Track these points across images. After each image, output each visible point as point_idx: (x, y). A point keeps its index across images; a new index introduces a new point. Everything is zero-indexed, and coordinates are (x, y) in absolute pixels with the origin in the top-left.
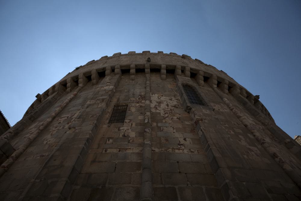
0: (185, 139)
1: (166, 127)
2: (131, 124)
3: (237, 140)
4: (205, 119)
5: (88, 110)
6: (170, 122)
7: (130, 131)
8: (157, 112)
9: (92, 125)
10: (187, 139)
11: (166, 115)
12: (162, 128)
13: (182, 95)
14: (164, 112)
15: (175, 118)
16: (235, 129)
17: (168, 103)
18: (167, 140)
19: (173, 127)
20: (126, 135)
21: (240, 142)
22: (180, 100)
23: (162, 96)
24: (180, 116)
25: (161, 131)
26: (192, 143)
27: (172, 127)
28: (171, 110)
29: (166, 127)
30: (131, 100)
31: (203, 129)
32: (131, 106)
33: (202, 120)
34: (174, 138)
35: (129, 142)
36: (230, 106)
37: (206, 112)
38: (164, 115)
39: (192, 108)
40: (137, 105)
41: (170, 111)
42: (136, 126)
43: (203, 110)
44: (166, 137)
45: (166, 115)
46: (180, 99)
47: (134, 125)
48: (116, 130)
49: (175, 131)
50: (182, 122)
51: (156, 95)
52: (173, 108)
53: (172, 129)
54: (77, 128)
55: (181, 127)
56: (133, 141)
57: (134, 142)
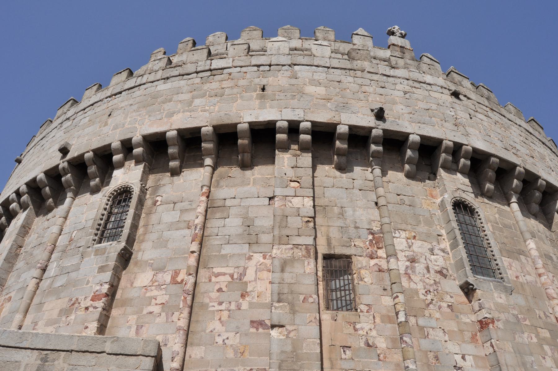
0: (463, 358)
1: (433, 328)
2: (371, 317)
3: (540, 357)
4: (498, 320)
5: (288, 277)
6: (438, 315)
7: (374, 333)
8: (411, 289)
9: (314, 324)
10: (467, 357)
11: (429, 297)
12: (425, 329)
13: (454, 246)
14: (425, 288)
15: (444, 305)
16: (539, 330)
17: (429, 262)
18: (437, 358)
19: (443, 330)
20: (371, 344)
21: (543, 361)
22: (448, 254)
23: (414, 237)
24: (452, 300)
25: (425, 338)
26: (474, 365)
27: (442, 328)
28: (436, 283)
29: (433, 328)
30: (355, 245)
31: (496, 344)
32: (359, 266)
33: (493, 322)
34: (447, 354)
35: (379, 360)
36: (538, 266)
37: (500, 301)
38: (425, 298)
39: (476, 289)
40: (373, 262)
41: (435, 287)
42: (382, 322)
43: (496, 295)
44: (435, 352)
45: (429, 297)
46: (448, 249)
47: (378, 320)
48: (351, 330)
49: (447, 338)
50: (457, 317)
51: (403, 234)
52: (438, 277)
53: (441, 333)
54: (288, 327)
55: (456, 330)
56: (385, 358)
57: (387, 360)
